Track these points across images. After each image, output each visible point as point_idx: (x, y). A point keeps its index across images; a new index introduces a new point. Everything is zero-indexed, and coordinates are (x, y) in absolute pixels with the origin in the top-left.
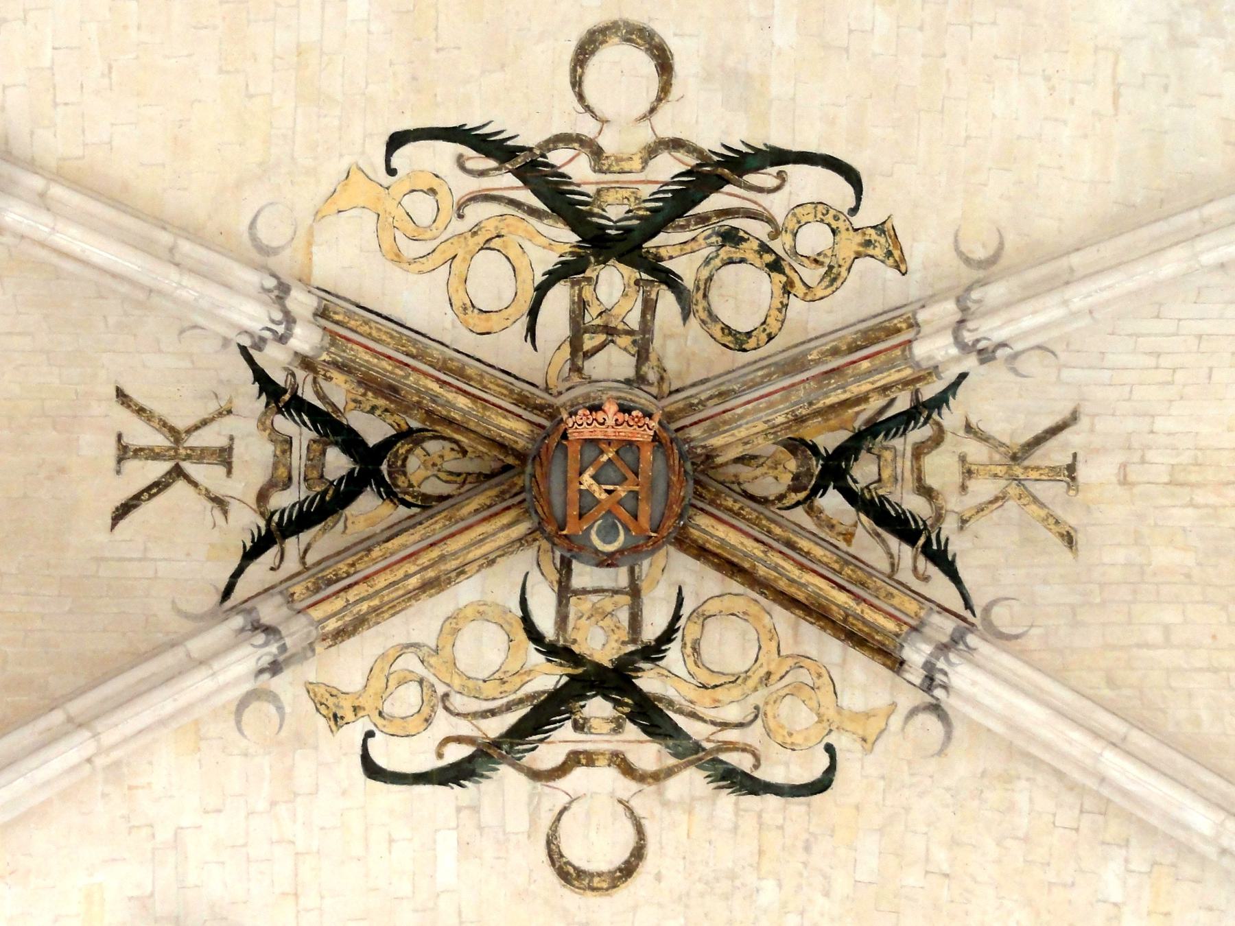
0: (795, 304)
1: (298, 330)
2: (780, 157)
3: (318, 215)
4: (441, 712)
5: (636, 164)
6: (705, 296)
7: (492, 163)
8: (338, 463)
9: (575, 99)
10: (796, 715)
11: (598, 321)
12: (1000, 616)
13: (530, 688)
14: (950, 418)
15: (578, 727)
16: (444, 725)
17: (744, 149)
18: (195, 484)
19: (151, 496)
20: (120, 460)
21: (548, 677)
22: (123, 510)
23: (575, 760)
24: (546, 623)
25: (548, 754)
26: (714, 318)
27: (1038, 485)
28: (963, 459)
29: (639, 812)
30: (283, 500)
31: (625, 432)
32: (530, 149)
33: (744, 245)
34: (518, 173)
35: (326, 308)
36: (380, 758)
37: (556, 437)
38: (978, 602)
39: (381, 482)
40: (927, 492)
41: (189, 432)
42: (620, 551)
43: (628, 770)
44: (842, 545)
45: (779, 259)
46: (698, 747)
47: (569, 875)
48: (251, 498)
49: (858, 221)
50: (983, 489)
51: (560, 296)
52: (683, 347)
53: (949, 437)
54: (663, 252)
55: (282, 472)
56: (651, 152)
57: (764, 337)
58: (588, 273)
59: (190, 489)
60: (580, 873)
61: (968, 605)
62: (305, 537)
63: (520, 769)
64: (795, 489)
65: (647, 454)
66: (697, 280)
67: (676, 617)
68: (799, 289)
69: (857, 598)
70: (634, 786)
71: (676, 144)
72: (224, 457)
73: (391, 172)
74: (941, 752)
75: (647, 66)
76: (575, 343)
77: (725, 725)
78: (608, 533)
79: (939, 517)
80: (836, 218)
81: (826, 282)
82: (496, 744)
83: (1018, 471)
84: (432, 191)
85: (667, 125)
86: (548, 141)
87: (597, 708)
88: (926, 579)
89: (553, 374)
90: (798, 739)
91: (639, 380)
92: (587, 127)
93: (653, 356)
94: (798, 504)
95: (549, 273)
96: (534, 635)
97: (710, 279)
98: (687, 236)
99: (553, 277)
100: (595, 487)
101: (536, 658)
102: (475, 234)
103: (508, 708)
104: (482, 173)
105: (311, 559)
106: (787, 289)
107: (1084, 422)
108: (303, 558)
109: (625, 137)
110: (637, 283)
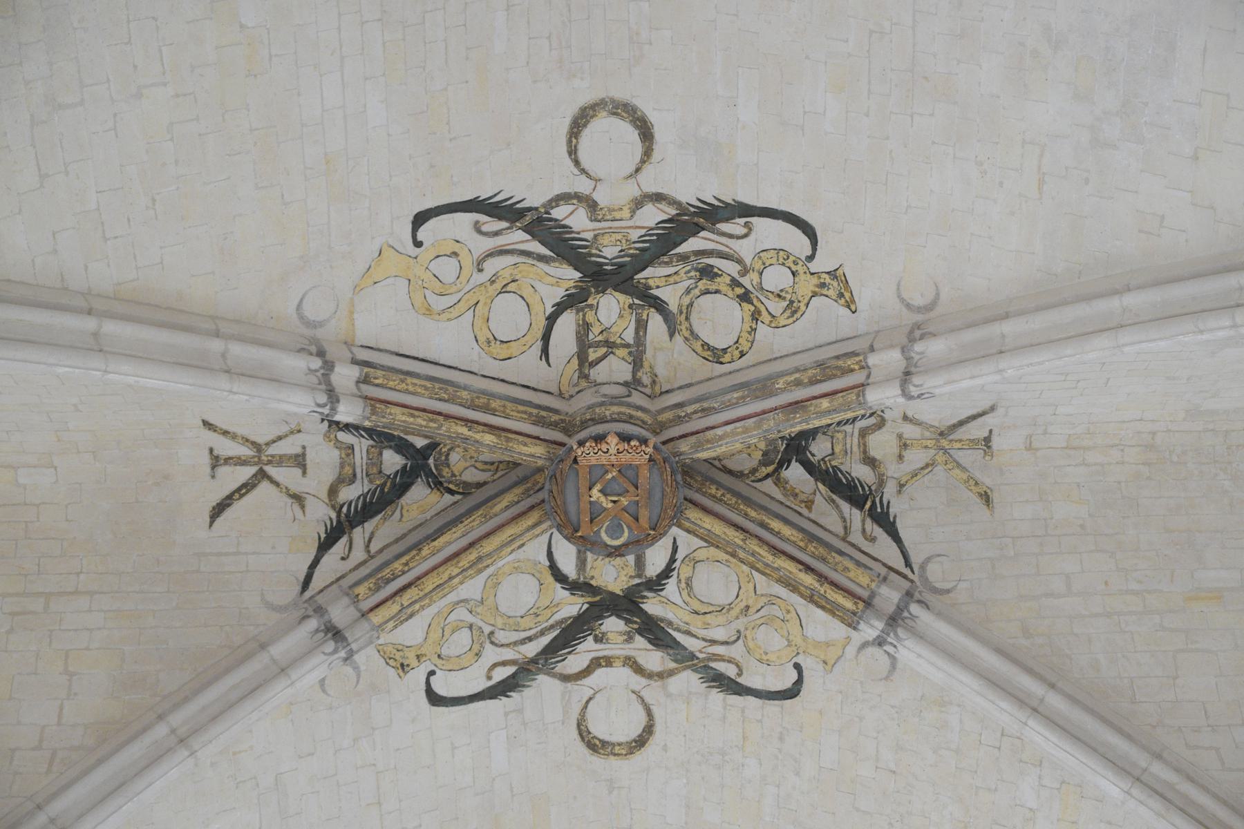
0: (762, 329)
1: (341, 408)
2: (747, 211)
3: (357, 289)
4: (488, 646)
5: (626, 213)
6: (687, 319)
7: (505, 224)
8: (392, 461)
9: (571, 164)
10: (770, 639)
11: (600, 338)
12: (935, 573)
13: (558, 617)
15: (598, 640)
16: (491, 654)
17: (716, 203)
18: (277, 484)
19: (242, 496)
20: (213, 467)
21: (572, 606)
22: (219, 509)
23: (596, 664)
24: (568, 566)
25: (575, 661)
26: (697, 337)
27: (960, 453)
28: (900, 436)
29: (648, 700)
31: (625, 458)
32: (536, 209)
33: (719, 279)
34: (526, 229)
35: (367, 376)
36: (440, 688)
37: (569, 462)
38: (916, 560)
39: (429, 474)
40: (871, 462)
41: (267, 444)
42: (625, 545)
43: (638, 669)
44: (805, 511)
45: (747, 292)
46: (693, 656)
47: (595, 746)
48: (324, 495)
49: (814, 266)
50: (916, 457)
51: (567, 324)
52: (669, 356)
53: (888, 425)
54: (651, 282)
55: (348, 470)
56: (638, 204)
57: (737, 353)
58: (590, 301)
59: (272, 488)
60: (604, 744)
61: (908, 564)
62: (369, 526)
63: (554, 676)
64: (764, 463)
65: (645, 472)
66: (680, 306)
67: (673, 560)
68: (765, 317)
69: (822, 577)
70: (644, 681)
71: (658, 198)
72: (300, 461)
73: (418, 244)
74: (887, 678)
75: (633, 135)
76: (582, 356)
77: (714, 642)
78: (615, 531)
79: (881, 483)
80: (795, 263)
81: (788, 313)
82: (534, 661)
83: (944, 443)
84: (455, 254)
85: (650, 181)
86: (551, 201)
87: (613, 625)
88: (873, 540)
89: (565, 381)
90: (772, 657)
91: (633, 384)
92: (583, 186)
93: (646, 364)
94: (768, 476)
95: (558, 304)
97: (691, 304)
98: (671, 270)
99: (560, 308)
100: (603, 499)
101: (562, 593)
102: (494, 282)
103: (542, 633)
104: (496, 234)
105: (374, 547)
106: (756, 316)
107: (1000, 411)
108: (368, 546)
109: (616, 192)
110: (630, 306)
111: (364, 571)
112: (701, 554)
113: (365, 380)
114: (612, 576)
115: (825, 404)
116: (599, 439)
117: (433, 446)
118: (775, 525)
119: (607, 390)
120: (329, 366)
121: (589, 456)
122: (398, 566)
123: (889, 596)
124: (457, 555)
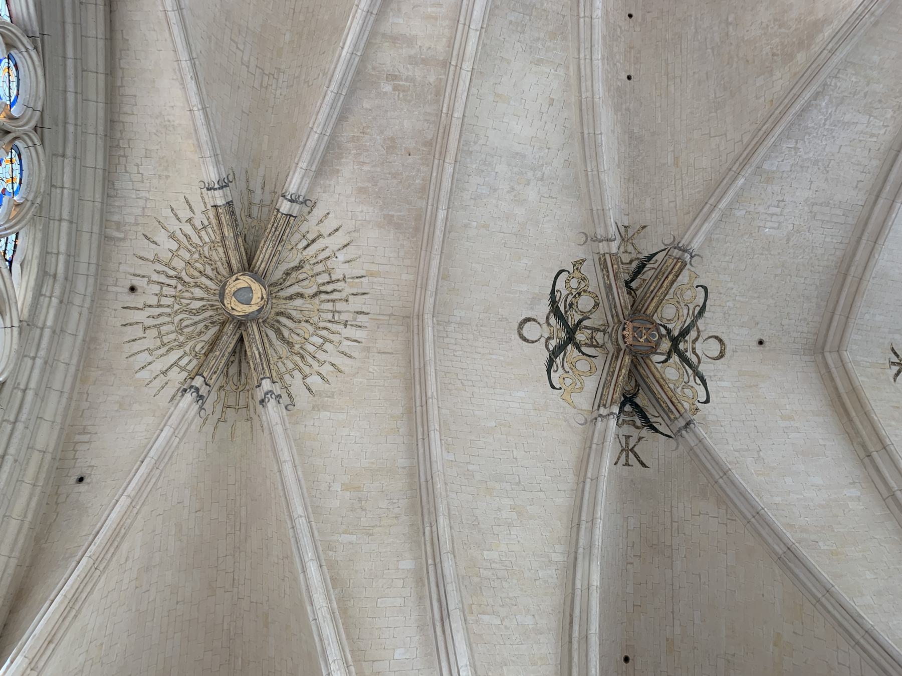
2: (553, 291)
8: (628, 408)
10: (688, 295)
16: (692, 383)
21: (675, 358)
24: (663, 358)
25: (694, 359)
30: (638, 423)
31: (631, 330)
36: (705, 399)
39: (632, 397)
40: (631, 262)
43: (697, 339)
47: (722, 355)
50: (630, 248)
51: (584, 349)
56: (549, 325)
62: (649, 416)
65: (635, 324)
69: (670, 273)
71: (547, 318)
72: (628, 437)
75: (529, 323)
78: (654, 336)
79: (638, 259)
85: (543, 320)
87: (681, 346)
91: (604, 331)
92: (543, 340)
96: (666, 361)
99: (580, 351)
106: (585, 291)
111: (666, 417)
112: (660, 316)
113: (605, 406)
114: (666, 345)
115: (615, 266)
116: (624, 337)
117: (624, 395)
118: (652, 288)
119: (606, 340)
120: (600, 415)
121: (629, 340)
122: (664, 405)
123: (676, 253)
124: (661, 386)
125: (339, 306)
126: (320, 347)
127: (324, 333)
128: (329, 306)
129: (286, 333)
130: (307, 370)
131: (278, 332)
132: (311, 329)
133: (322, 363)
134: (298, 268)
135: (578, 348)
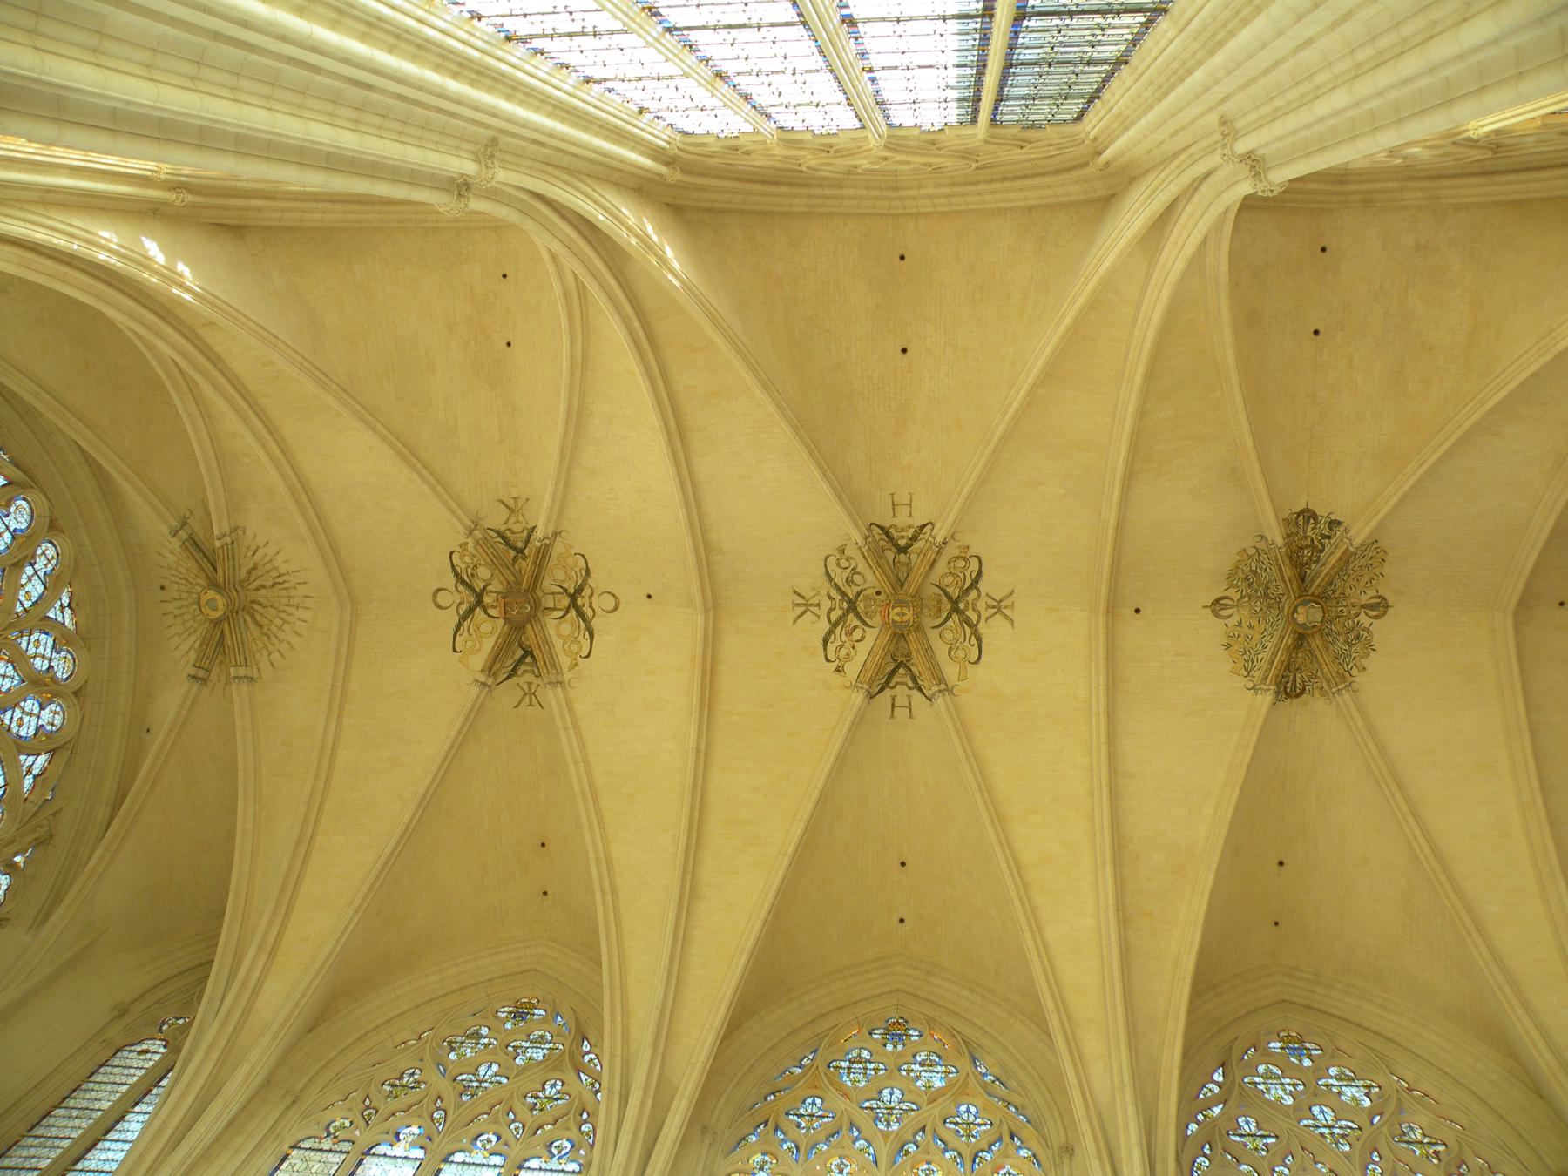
10: (570, 561)
14: (502, 528)
16: (580, 638)
21: (573, 613)
24: (561, 613)
25: (589, 613)
47: (616, 608)
51: (491, 611)
72: (529, 684)
87: (579, 601)
109: (455, 598)
125: (292, 592)
126: (280, 628)
127: (283, 615)
128: (284, 593)
129: (258, 617)
130: (271, 648)
131: (253, 617)
132: (274, 612)
133: (281, 641)
134: (254, 568)
135: (485, 610)
